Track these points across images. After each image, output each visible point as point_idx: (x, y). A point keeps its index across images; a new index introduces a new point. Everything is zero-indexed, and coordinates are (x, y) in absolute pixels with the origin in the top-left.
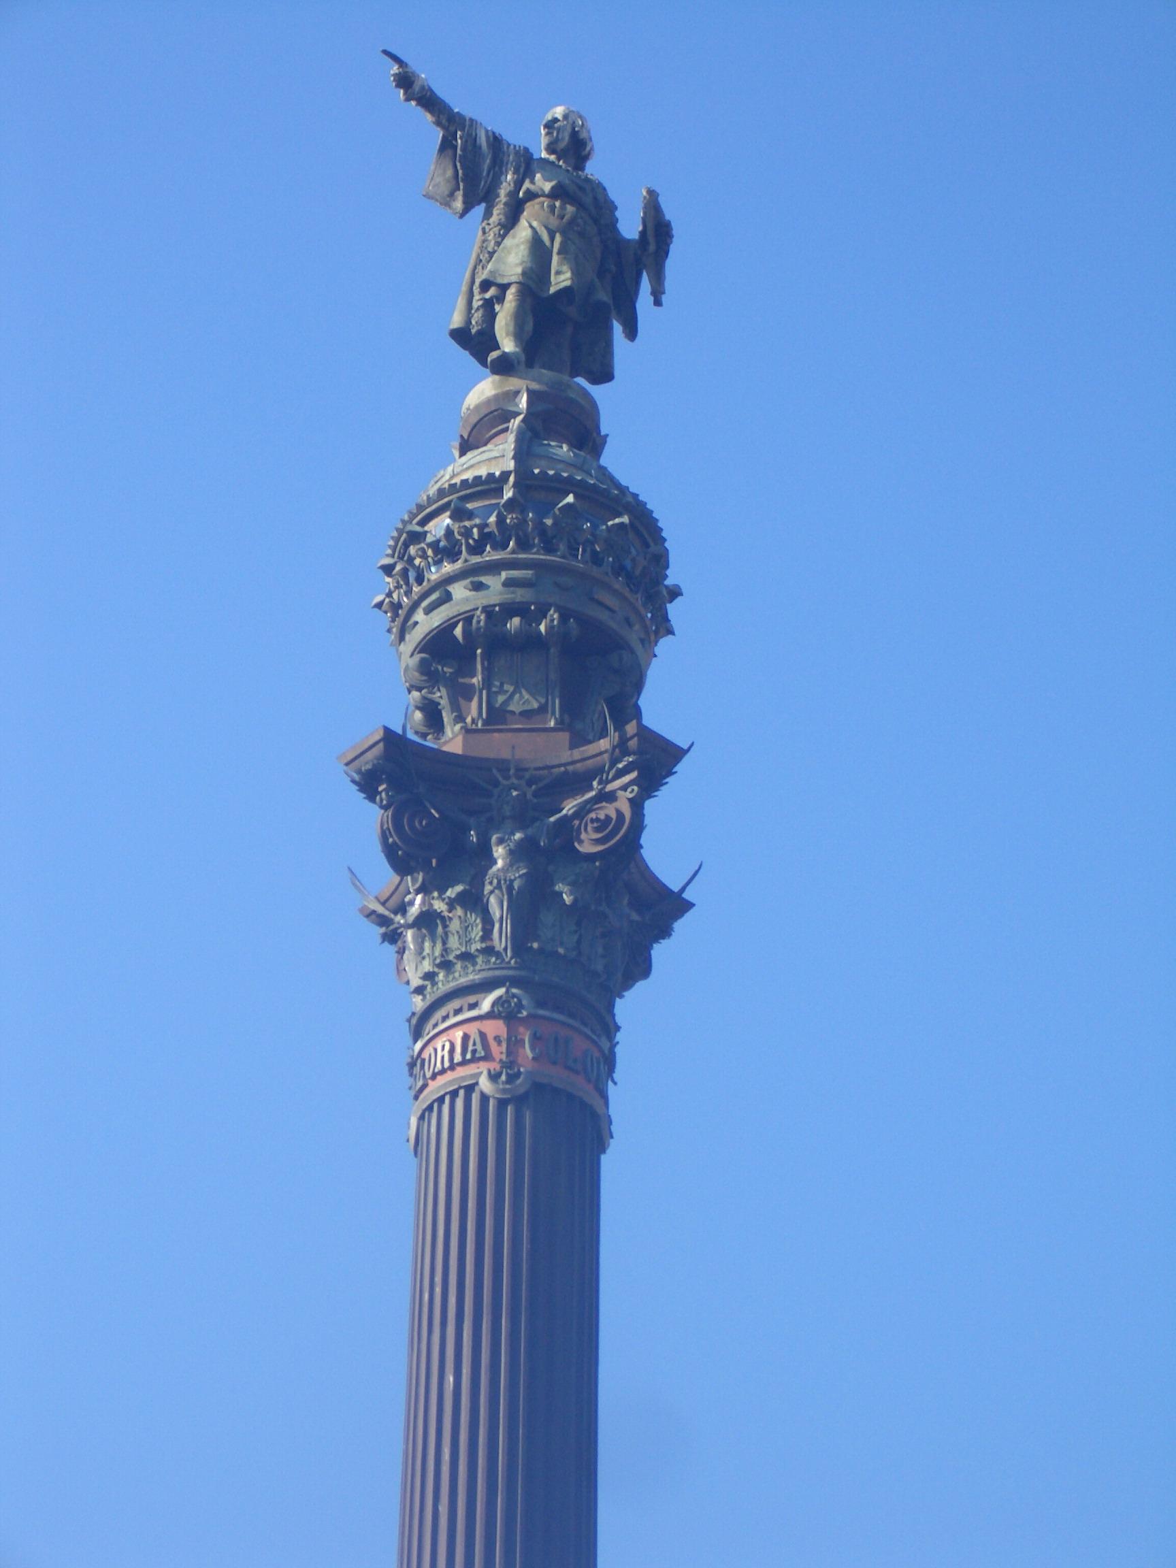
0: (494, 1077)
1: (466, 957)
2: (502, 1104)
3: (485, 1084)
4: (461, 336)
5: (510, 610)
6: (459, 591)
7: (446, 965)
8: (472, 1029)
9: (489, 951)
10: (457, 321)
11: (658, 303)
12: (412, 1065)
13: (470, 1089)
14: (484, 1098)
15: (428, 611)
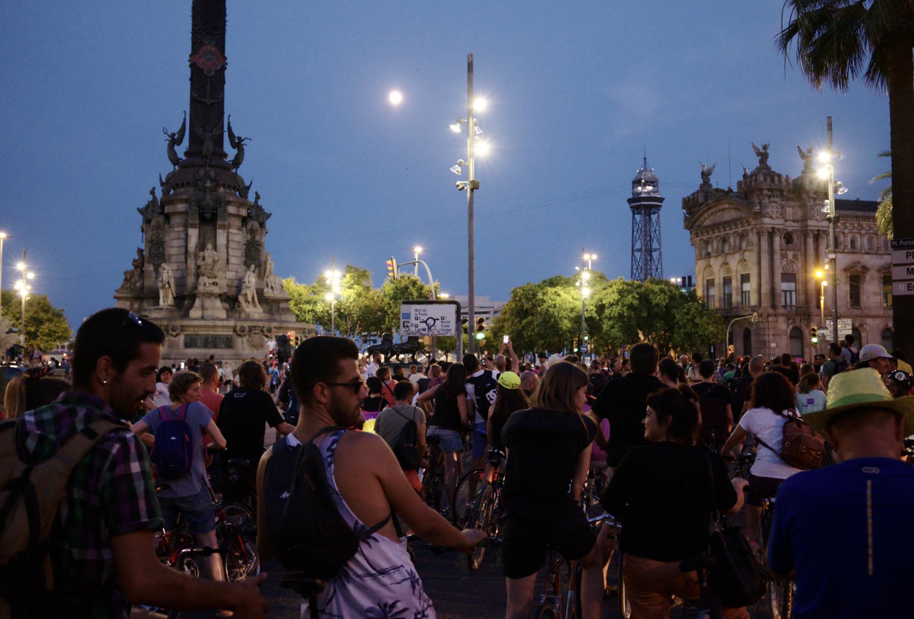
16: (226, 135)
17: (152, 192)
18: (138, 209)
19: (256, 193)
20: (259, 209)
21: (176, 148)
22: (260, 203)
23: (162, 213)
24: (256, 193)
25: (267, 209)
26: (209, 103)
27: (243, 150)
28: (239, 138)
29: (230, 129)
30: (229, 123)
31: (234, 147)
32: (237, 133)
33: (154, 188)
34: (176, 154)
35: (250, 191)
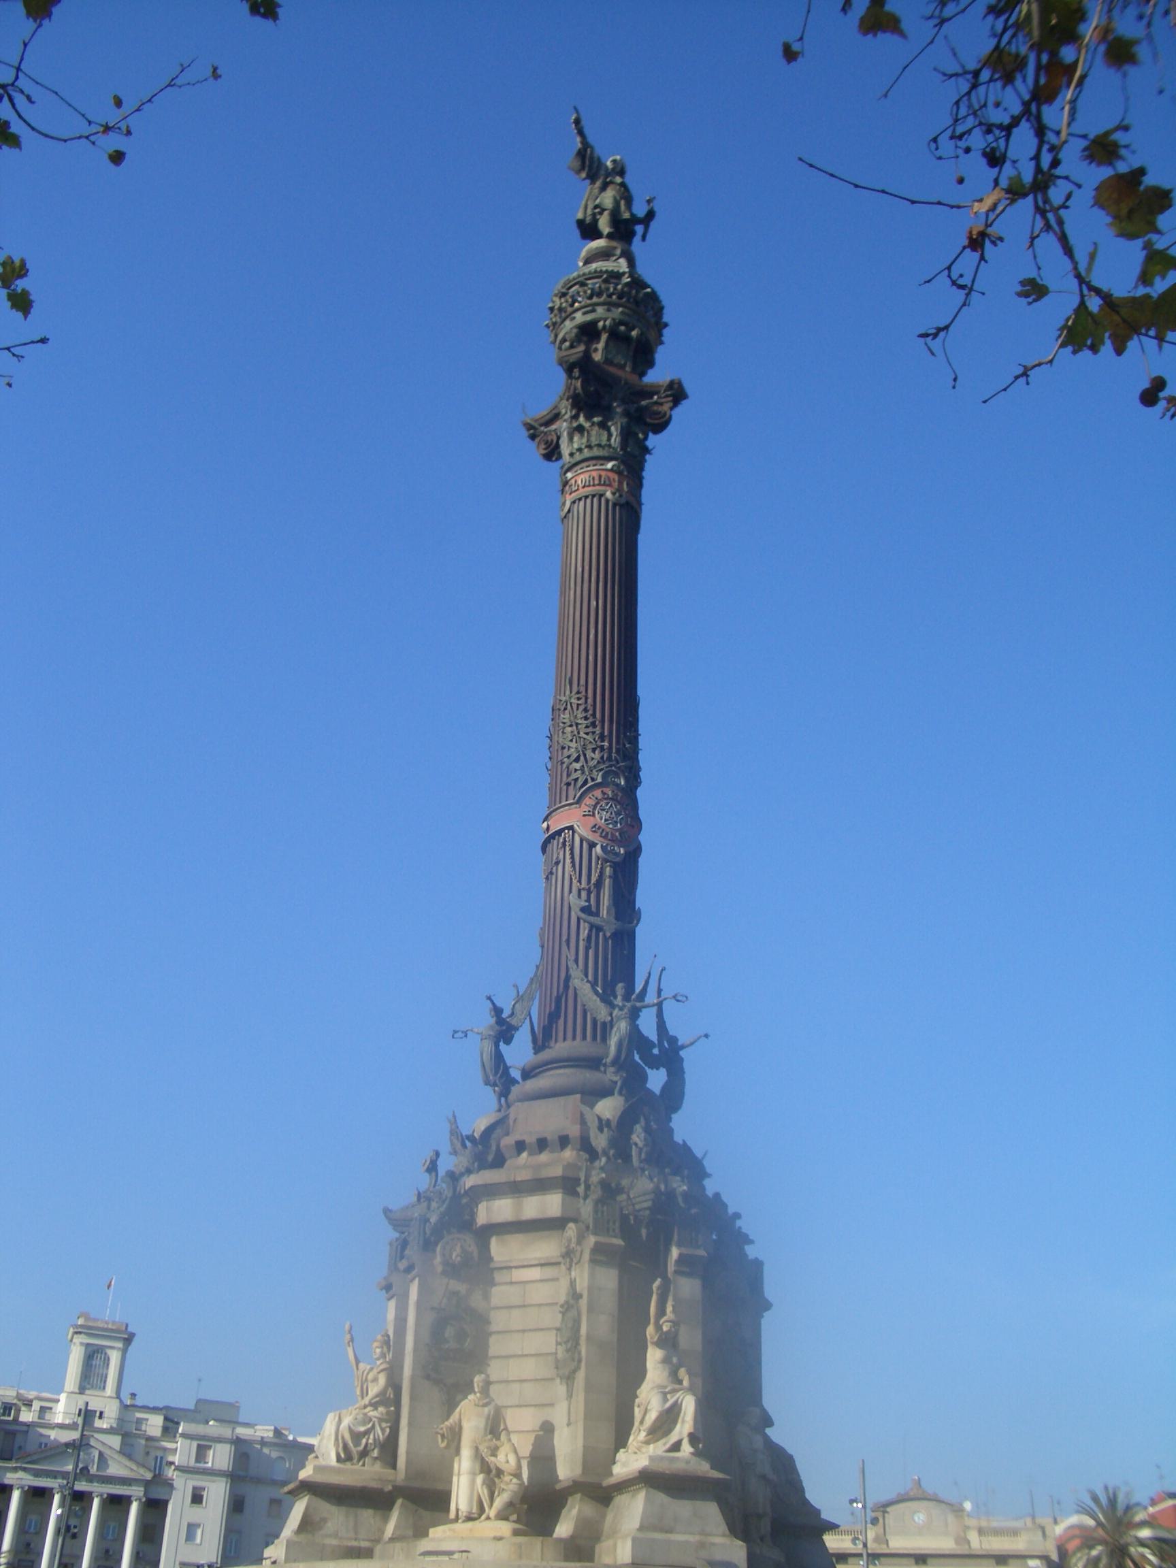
0: (614, 494)
1: (599, 445)
2: (615, 505)
3: (609, 494)
4: (581, 223)
5: (621, 323)
6: (600, 310)
7: (589, 447)
8: (603, 474)
9: (610, 446)
10: (580, 216)
11: (644, 238)
12: (566, 483)
13: (601, 496)
14: (607, 501)
15: (584, 313)
18: (387, 1212)
21: (502, 1046)
30: (659, 991)
33: (437, 1154)
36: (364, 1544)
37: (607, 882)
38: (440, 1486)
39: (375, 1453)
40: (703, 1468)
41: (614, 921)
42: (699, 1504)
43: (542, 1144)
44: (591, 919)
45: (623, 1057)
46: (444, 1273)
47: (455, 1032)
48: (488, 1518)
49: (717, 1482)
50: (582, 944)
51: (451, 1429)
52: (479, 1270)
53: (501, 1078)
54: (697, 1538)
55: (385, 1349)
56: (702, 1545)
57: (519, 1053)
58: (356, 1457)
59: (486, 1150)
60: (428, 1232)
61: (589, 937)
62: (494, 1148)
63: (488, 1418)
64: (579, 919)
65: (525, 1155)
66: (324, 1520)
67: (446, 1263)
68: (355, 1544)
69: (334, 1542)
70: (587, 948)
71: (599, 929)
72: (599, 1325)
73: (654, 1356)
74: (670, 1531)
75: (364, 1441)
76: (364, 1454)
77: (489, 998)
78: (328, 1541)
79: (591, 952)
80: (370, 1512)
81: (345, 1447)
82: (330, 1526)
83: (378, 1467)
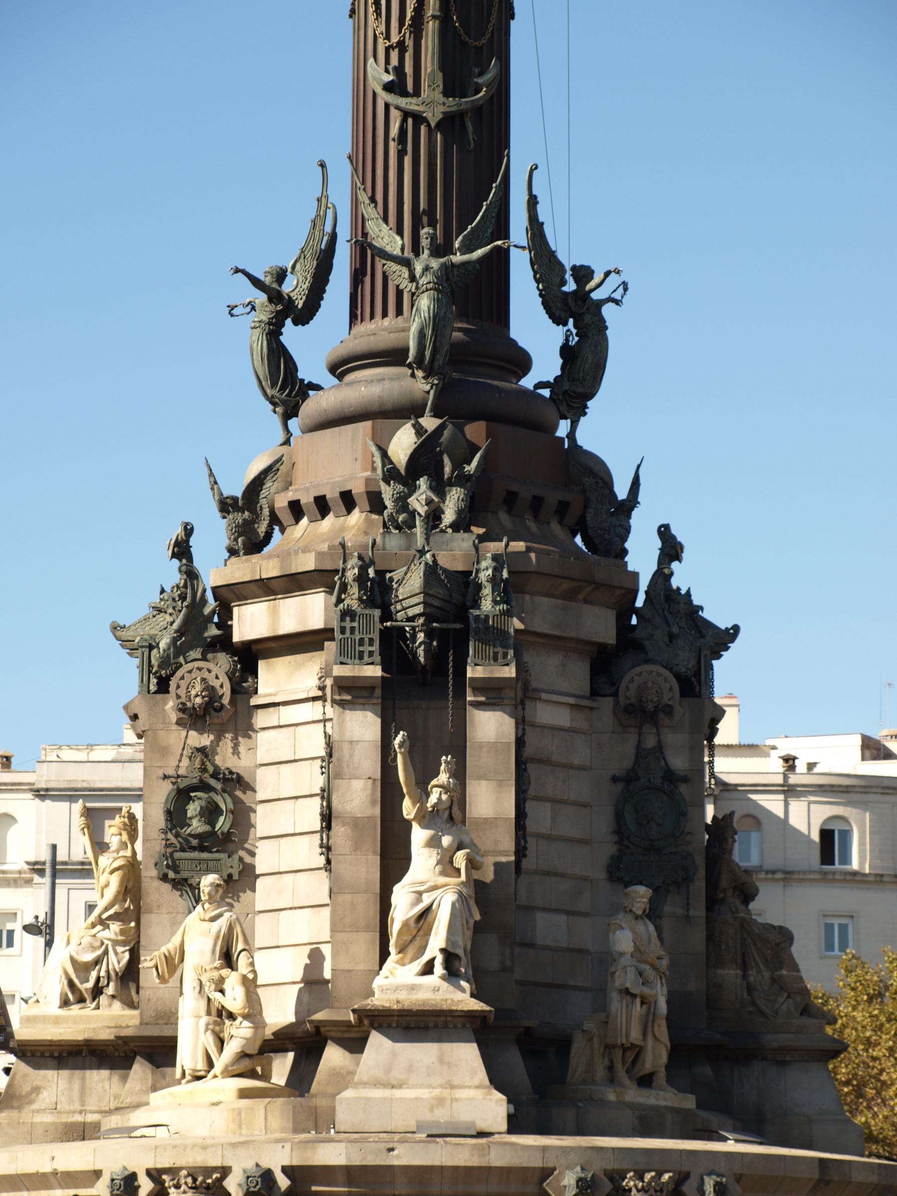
16: (520, 266)
17: (182, 550)
18: (115, 628)
19: (665, 532)
20: (672, 604)
21: (290, 334)
22: (682, 577)
23: (224, 643)
24: (665, 532)
25: (717, 614)
26: (434, 116)
27: (602, 326)
28: (583, 274)
29: (536, 228)
31: (559, 321)
32: (569, 255)
34: (291, 367)
35: (637, 518)
36: (91, 1118)
37: (431, 28)
38: (167, 1032)
39: (111, 990)
40: (462, 998)
41: (442, 99)
42: (447, 1046)
43: (322, 506)
44: (403, 102)
45: (428, 353)
46: (179, 723)
47: (232, 308)
48: (215, 1076)
49: (470, 1015)
50: (393, 146)
51: (168, 959)
52: (229, 712)
53: (286, 387)
54: (437, 1092)
55: (125, 837)
56: (440, 1101)
57: (312, 346)
58: (88, 997)
59: (251, 517)
60: (154, 662)
61: (403, 132)
62: (266, 512)
63: (217, 938)
64: (387, 106)
65: (305, 521)
66: (37, 1090)
67: (183, 709)
68: (79, 1118)
69: (49, 1118)
70: (401, 154)
71: (418, 119)
72: (358, 797)
73: (419, 835)
74: (400, 1086)
75: (94, 974)
76: (97, 991)
77: (237, 271)
78: (38, 1119)
79: (408, 161)
80: (105, 1073)
81: (71, 984)
82: (46, 1098)
83: (117, 1008)
